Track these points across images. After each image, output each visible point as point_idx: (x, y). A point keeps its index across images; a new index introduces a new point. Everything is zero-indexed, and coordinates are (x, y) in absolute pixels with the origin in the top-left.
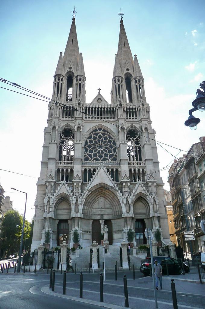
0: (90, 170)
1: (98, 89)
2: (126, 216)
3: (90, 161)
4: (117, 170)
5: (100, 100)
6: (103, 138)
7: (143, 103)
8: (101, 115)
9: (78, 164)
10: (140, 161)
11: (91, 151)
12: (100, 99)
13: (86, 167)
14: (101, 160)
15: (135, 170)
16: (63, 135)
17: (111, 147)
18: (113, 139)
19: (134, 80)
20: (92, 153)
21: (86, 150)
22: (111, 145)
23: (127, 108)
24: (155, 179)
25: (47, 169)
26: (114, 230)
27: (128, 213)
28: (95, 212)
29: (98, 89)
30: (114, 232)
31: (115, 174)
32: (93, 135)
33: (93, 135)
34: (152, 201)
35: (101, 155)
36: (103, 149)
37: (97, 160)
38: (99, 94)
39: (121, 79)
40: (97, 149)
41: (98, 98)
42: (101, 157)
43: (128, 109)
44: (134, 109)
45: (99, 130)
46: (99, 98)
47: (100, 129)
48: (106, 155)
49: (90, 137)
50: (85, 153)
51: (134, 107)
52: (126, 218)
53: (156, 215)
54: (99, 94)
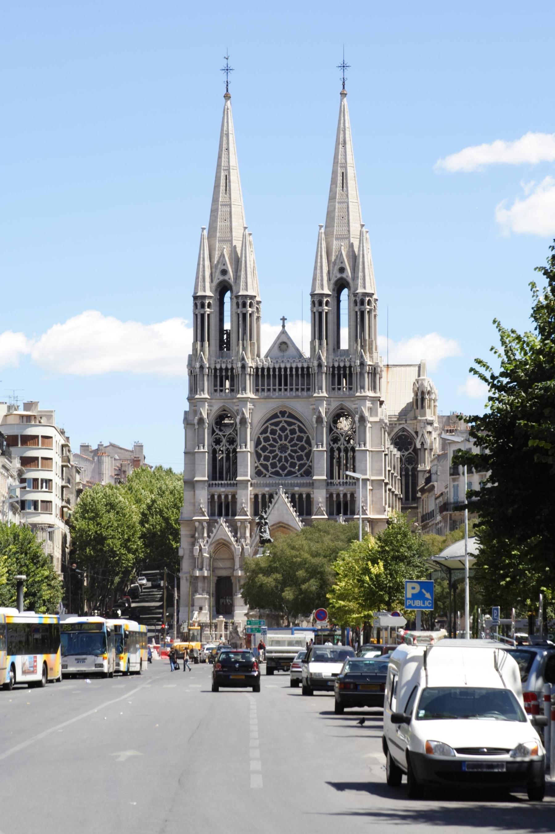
0: (264, 496)
1: (281, 319)
3: (265, 476)
4: (308, 495)
5: (284, 346)
8: (286, 385)
12: (284, 343)
14: (283, 475)
15: (338, 495)
16: (217, 428)
17: (302, 448)
18: (305, 433)
20: (268, 461)
23: (333, 367)
25: (194, 495)
29: (281, 319)
31: (303, 506)
32: (269, 426)
33: (269, 426)
37: (277, 474)
38: (284, 332)
41: (280, 341)
42: (283, 468)
43: (336, 369)
44: (348, 369)
45: (280, 416)
46: (283, 344)
47: (283, 413)
48: (293, 465)
49: (265, 431)
51: (347, 364)
54: (284, 332)
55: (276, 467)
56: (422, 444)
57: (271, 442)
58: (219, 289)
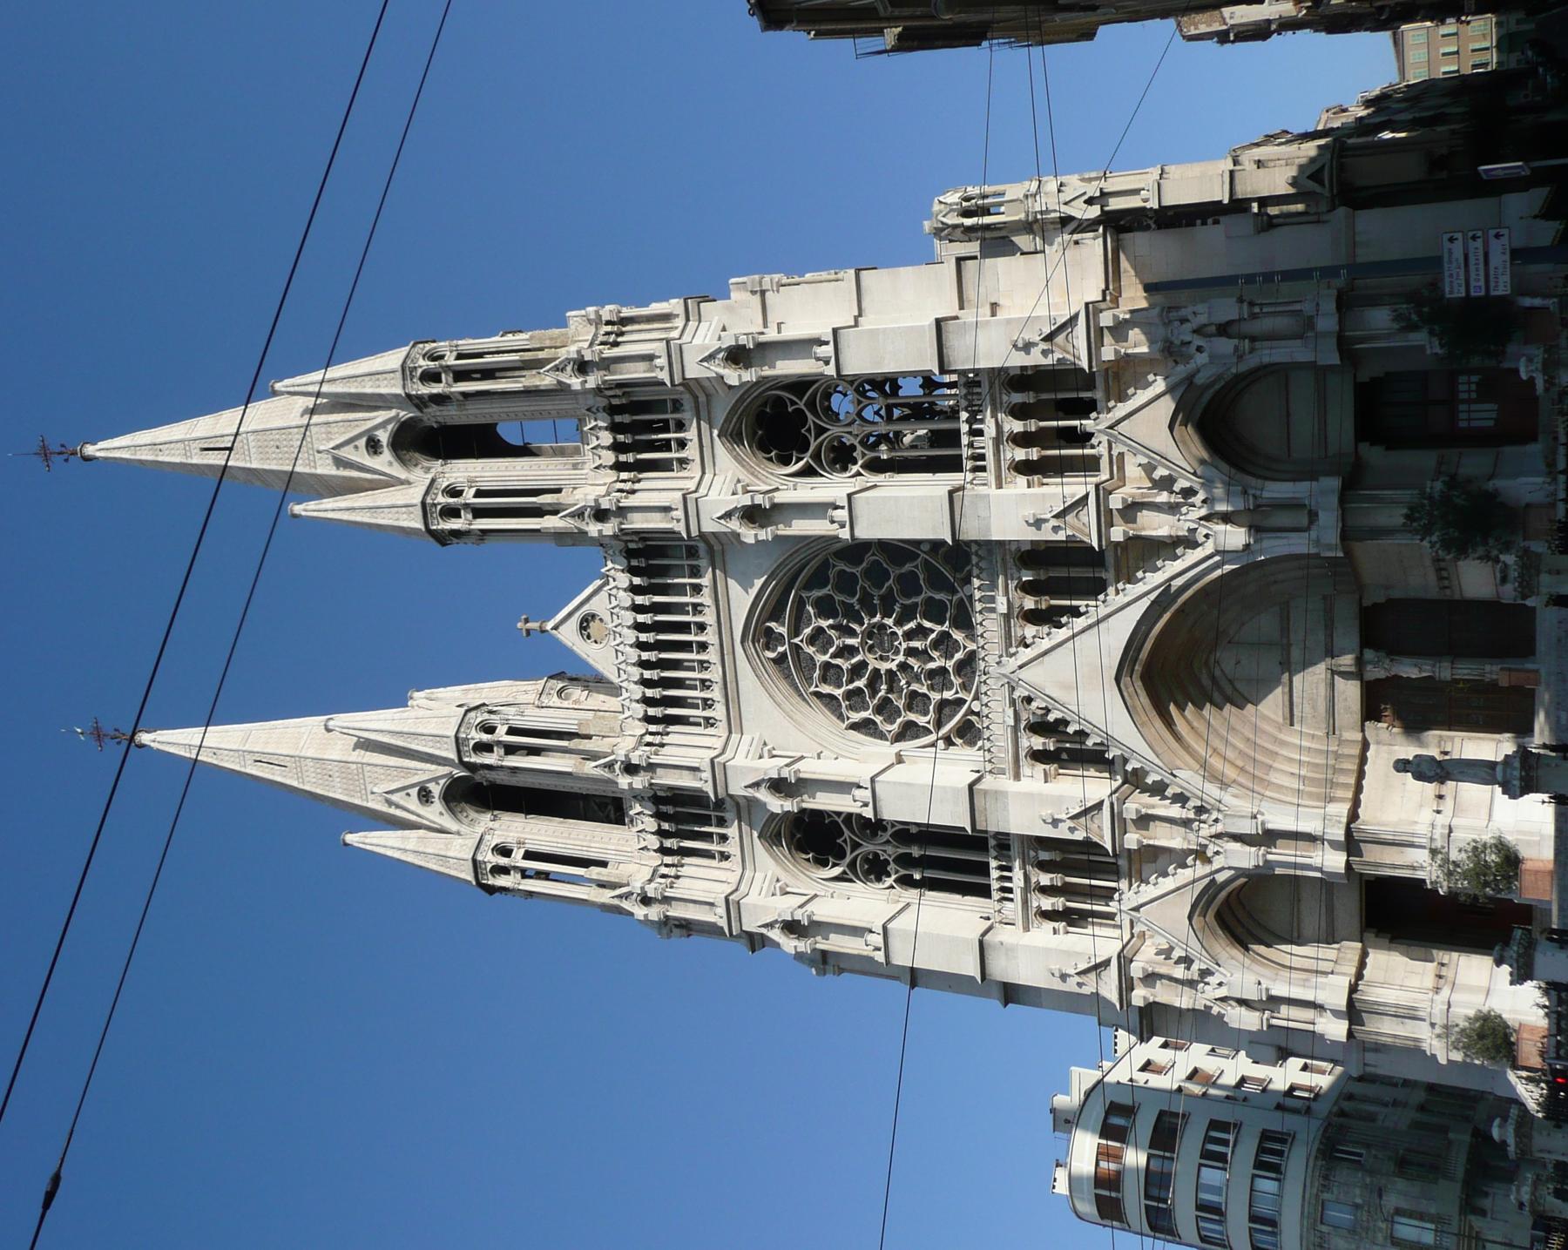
2: (1332, 537)
5: (594, 627)
6: (824, 623)
7: (569, 368)
9: (1005, 808)
10: (958, 444)
11: (916, 701)
13: (1022, 754)
17: (877, 575)
18: (825, 565)
19: (433, 410)
21: (909, 731)
22: (867, 573)
24: (1076, 316)
26: (1433, 593)
27: (1313, 516)
28: (1314, 708)
30: (1448, 592)
33: (812, 689)
34: (1226, 345)
35: (936, 645)
36: (900, 633)
39: (442, 500)
40: (903, 667)
50: (933, 745)
52: (1346, 536)
53: (1328, 322)
55: (943, 671)
56: (1090, 201)
57: (860, 683)
58: (473, 814)
